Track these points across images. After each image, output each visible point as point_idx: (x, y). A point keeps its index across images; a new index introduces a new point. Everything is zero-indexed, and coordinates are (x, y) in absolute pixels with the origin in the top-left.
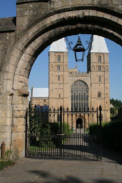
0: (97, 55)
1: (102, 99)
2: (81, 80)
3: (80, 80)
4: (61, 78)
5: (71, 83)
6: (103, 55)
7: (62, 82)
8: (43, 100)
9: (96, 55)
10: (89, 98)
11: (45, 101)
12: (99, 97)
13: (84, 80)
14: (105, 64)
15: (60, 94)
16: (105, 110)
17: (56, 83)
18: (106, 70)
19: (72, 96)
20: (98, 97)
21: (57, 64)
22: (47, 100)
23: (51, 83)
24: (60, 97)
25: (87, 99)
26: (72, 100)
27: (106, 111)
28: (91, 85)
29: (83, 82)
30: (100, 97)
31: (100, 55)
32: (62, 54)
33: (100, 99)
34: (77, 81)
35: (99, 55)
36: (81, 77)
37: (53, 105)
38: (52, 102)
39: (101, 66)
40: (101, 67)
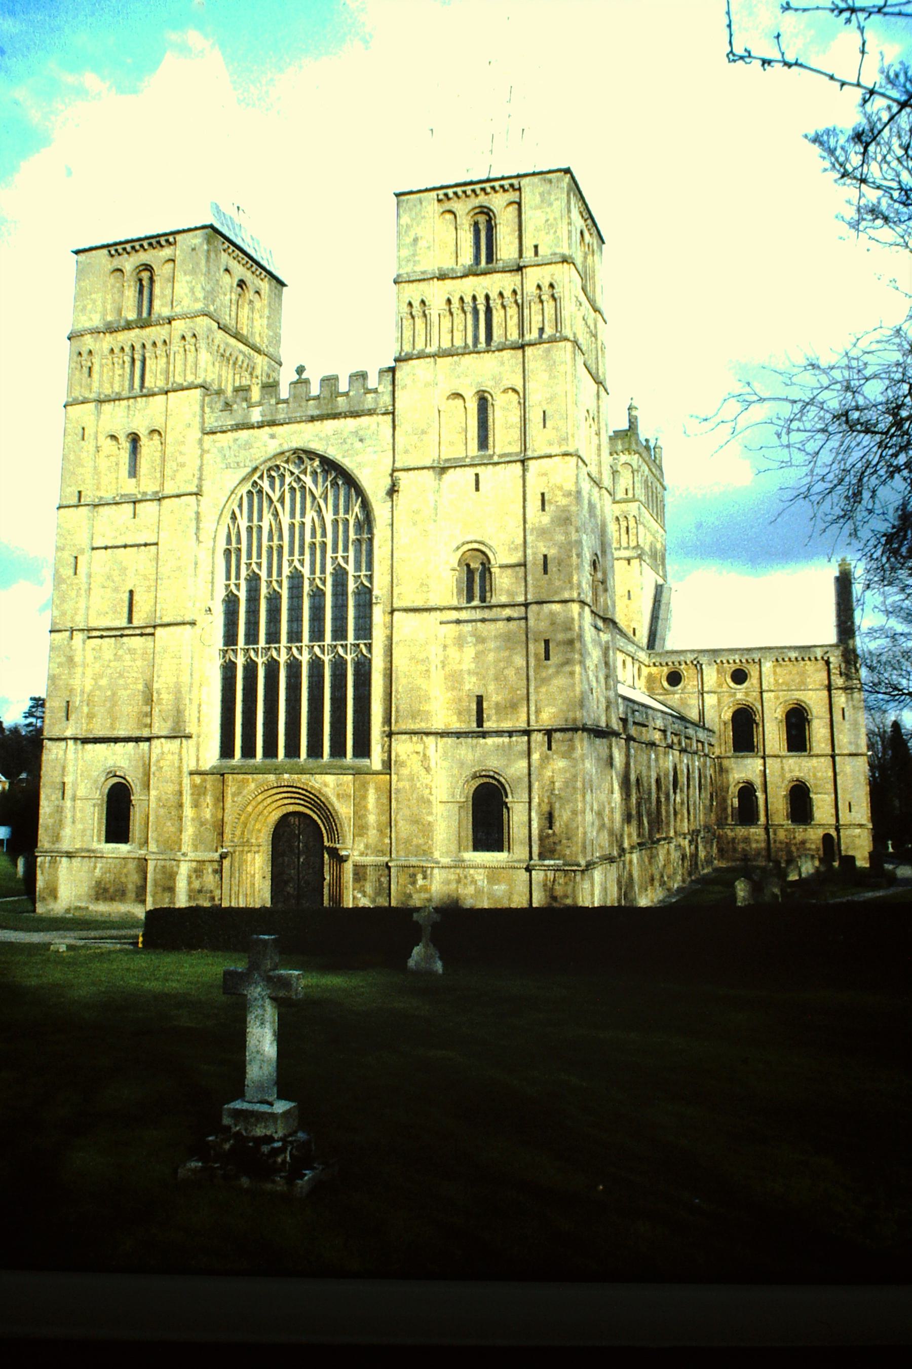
0: (455, 205)
1: (508, 612)
2: (311, 454)
4: (148, 447)
6: (513, 196)
9: (447, 205)
10: (379, 615)
12: (476, 602)
13: (333, 453)
14: (533, 276)
15: (131, 592)
18: (542, 330)
19: (231, 603)
20: (470, 598)
21: (134, 335)
25: (365, 630)
26: (230, 638)
29: (330, 466)
31: (482, 199)
32: (167, 252)
33: (478, 614)
34: (273, 471)
35: (476, 202)
36: (312, 419)
39: (495, 304)
40: (489, 311)
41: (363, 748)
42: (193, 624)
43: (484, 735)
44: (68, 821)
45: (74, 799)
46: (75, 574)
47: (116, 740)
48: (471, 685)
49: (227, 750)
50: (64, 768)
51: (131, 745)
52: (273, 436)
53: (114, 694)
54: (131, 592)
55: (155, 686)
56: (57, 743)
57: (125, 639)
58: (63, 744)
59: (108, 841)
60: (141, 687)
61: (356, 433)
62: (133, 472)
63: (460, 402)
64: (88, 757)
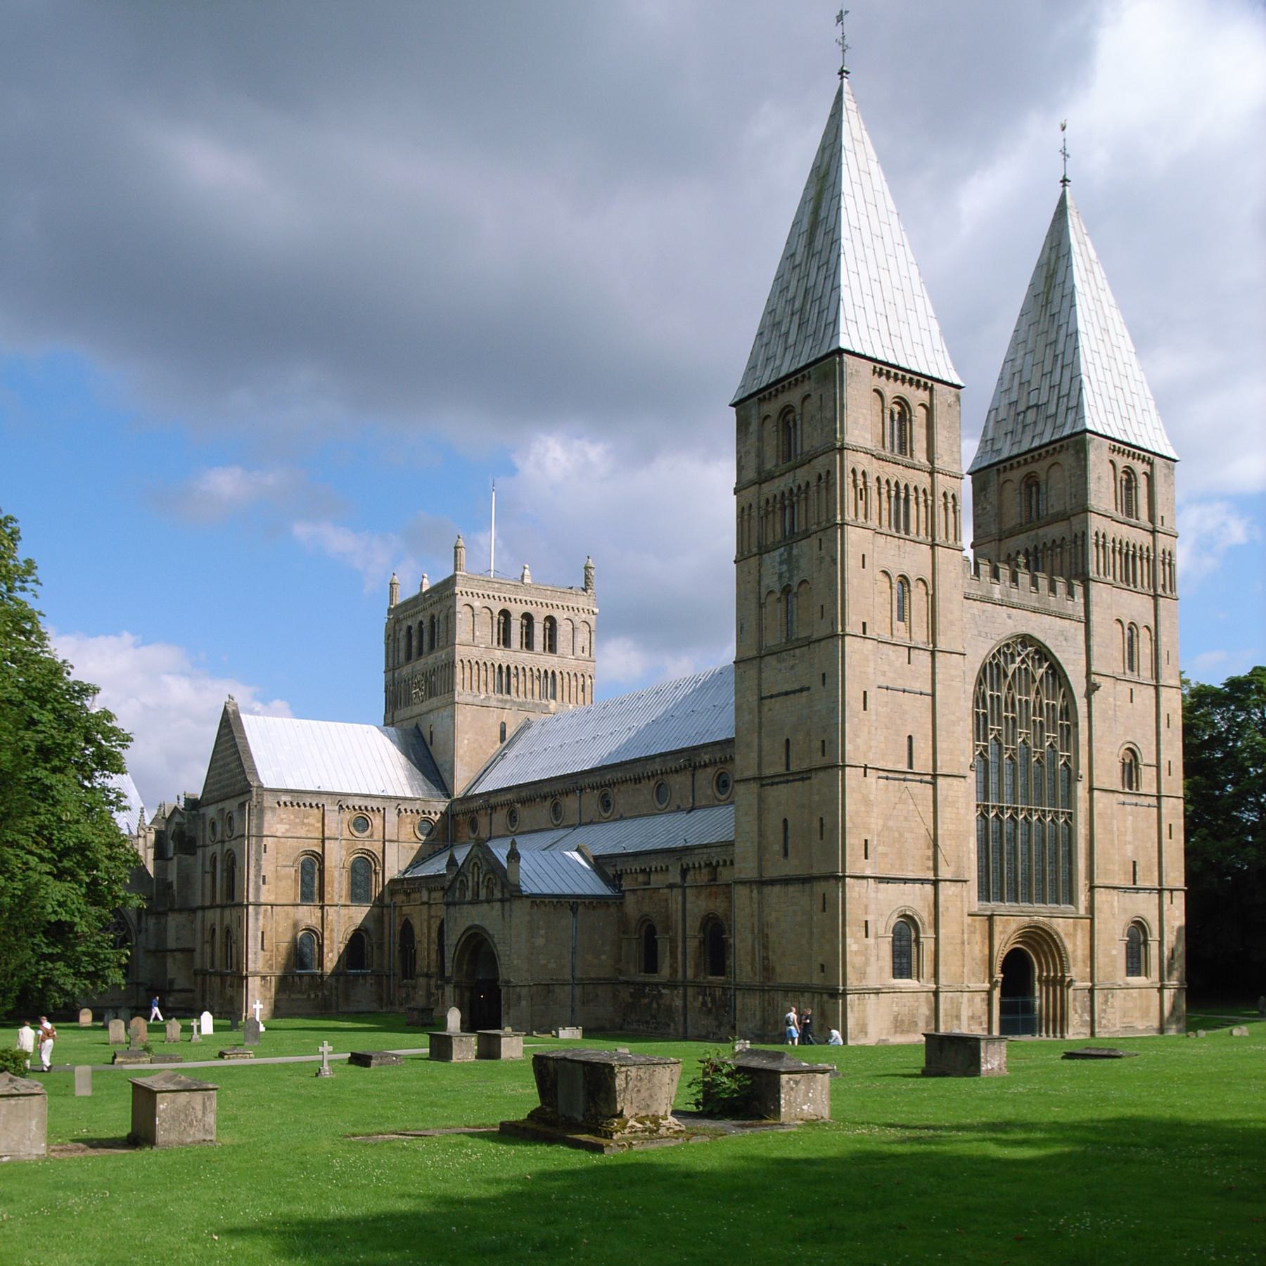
3: (1026, 640)
5: (980, 652)
7: (920, 636)
8: (348, 816)
10: (1081, 789)
11: (362, 823)
15: (910, 737)
16: (1160, 891)
17: (886, 636)
22: (376, 821)
23: (860, 632)
24: (911, 765)
27: (1166, 895)
28: (1092, 688)
30: (1131, 788)
33: (1134, 799)
37: (869, 831)
38: (867, 802)
41: (1071, 899)
42: (964, 777)
43: (1138, 890)
44: (873, 959)
45: (877, 937)
46: (865, 709)
47: (905, 881)
48: (1129, 851)
49: (984, 895)
50: (866, 907)
51: (918, 886)
52: (1010, 617)
53: (901, 835)
54: (910, 737)
55: (940, 832)
56: (860, 881)
57: (908, 783)
58: (865, 881)
59: (894, 977)
60: (923, 831)
61: (1062, 632)
62: (902, 613)
63: (1119, 626)
64: (881, 896)
